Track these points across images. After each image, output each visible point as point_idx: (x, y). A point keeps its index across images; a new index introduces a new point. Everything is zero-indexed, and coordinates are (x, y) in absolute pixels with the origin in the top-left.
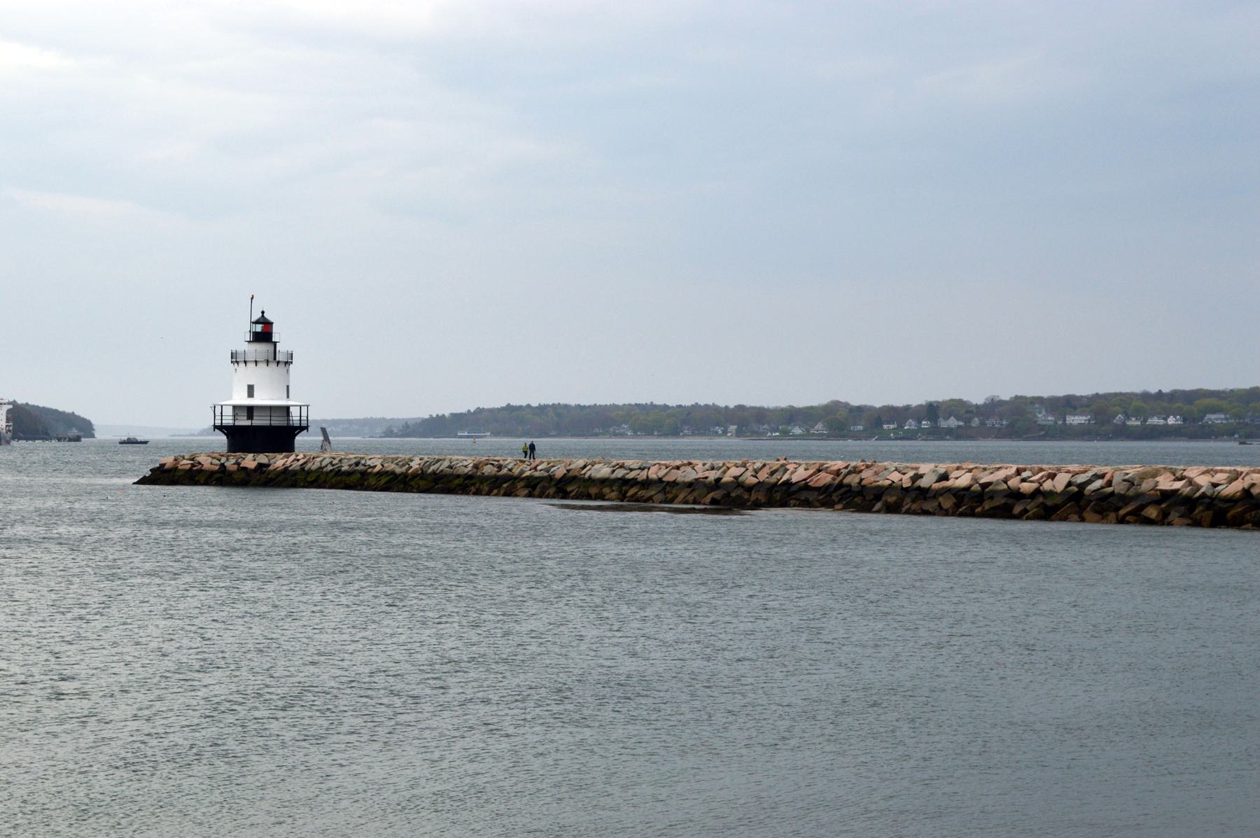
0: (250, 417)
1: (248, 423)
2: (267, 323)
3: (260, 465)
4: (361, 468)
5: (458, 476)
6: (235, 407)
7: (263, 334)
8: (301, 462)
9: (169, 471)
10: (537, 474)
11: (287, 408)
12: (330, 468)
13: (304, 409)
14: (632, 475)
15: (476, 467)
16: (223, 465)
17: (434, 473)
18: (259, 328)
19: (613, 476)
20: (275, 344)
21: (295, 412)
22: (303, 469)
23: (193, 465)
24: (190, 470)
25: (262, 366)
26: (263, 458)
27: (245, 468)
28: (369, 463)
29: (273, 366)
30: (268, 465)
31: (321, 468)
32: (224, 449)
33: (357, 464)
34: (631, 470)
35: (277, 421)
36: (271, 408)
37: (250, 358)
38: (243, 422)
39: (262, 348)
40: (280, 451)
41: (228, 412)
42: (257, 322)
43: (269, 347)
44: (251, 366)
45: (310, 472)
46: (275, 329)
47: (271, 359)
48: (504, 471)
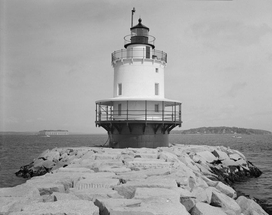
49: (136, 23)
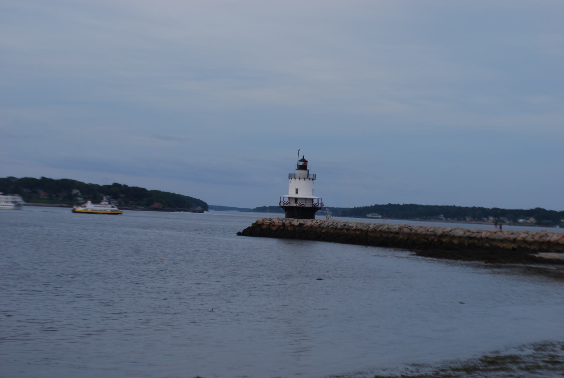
0: (296, 202)
1: (295, 205)
2: (303, 160)
3: (300, 224)
4: (346, 227)
5: (392, 233)
6: (289, 198)
7: (303, 166)
8: (319, 223)
9: (260, 225)
10: (429, 233)
11: (312, 199)
12: (332, 226)
13: (320, 200)
14: (474, 235)
15: (400, 229)
16: (284, 223)
17: (380, 231)
18: (301, 163)
19: (465, 235)
20: (308, 171)
21: (315, 201)
22: (320, 227)
23: (271, 223)
24: (269, 225)
25: (302, 180)
26: (301, 221)
27: (294, 225)
28: (350, 225)
29: (307, 180)
30: (304, 224)
31: (328, 226)
32: (284, 217)
33: (345, 225)
34: (473, 233)
35: (308, 205)
36: (305, 199)
37: (297, 176)
38: (293, 204)
39: (303, 172)
40: (309, 218)
41: (286, 200)
42: (301, 161)
43: (306, 172)
44: (297, 180)
45: (323, 228)
46: (309, 164)
47: (306, 177)
48: (413, 231)
49: (301, 158)
